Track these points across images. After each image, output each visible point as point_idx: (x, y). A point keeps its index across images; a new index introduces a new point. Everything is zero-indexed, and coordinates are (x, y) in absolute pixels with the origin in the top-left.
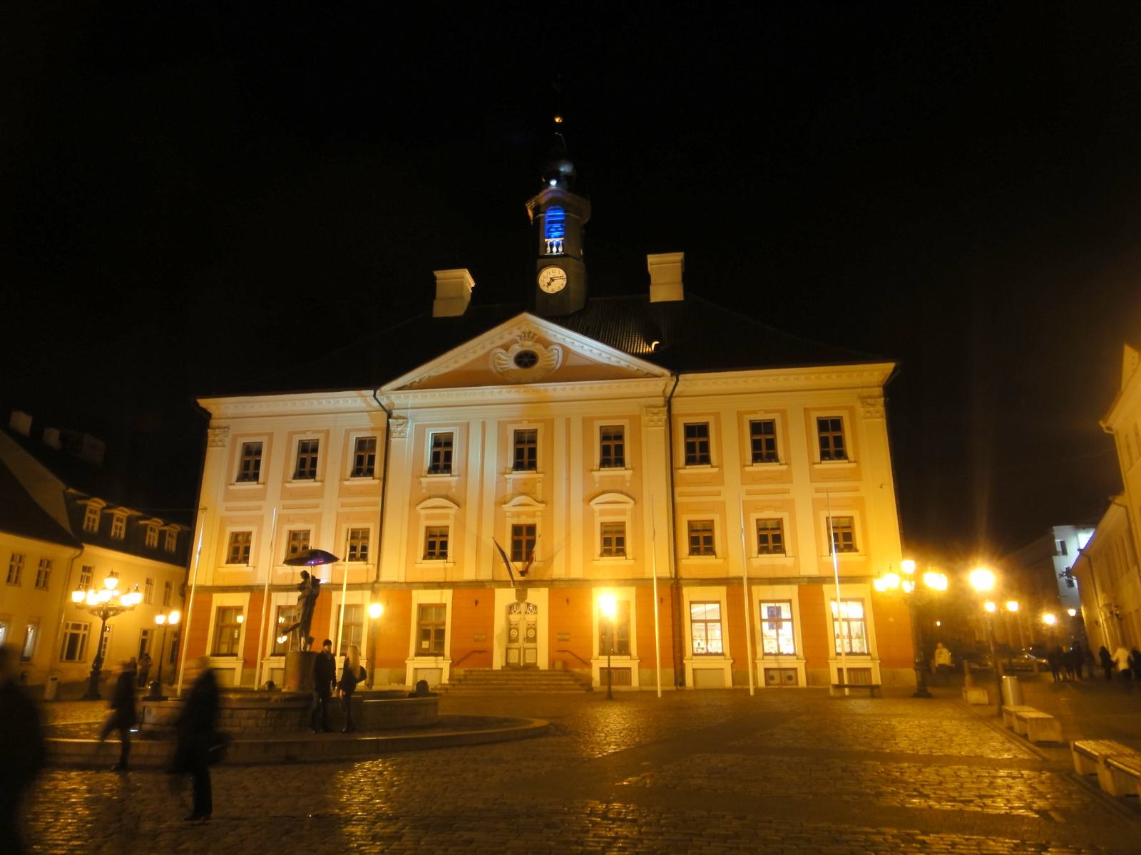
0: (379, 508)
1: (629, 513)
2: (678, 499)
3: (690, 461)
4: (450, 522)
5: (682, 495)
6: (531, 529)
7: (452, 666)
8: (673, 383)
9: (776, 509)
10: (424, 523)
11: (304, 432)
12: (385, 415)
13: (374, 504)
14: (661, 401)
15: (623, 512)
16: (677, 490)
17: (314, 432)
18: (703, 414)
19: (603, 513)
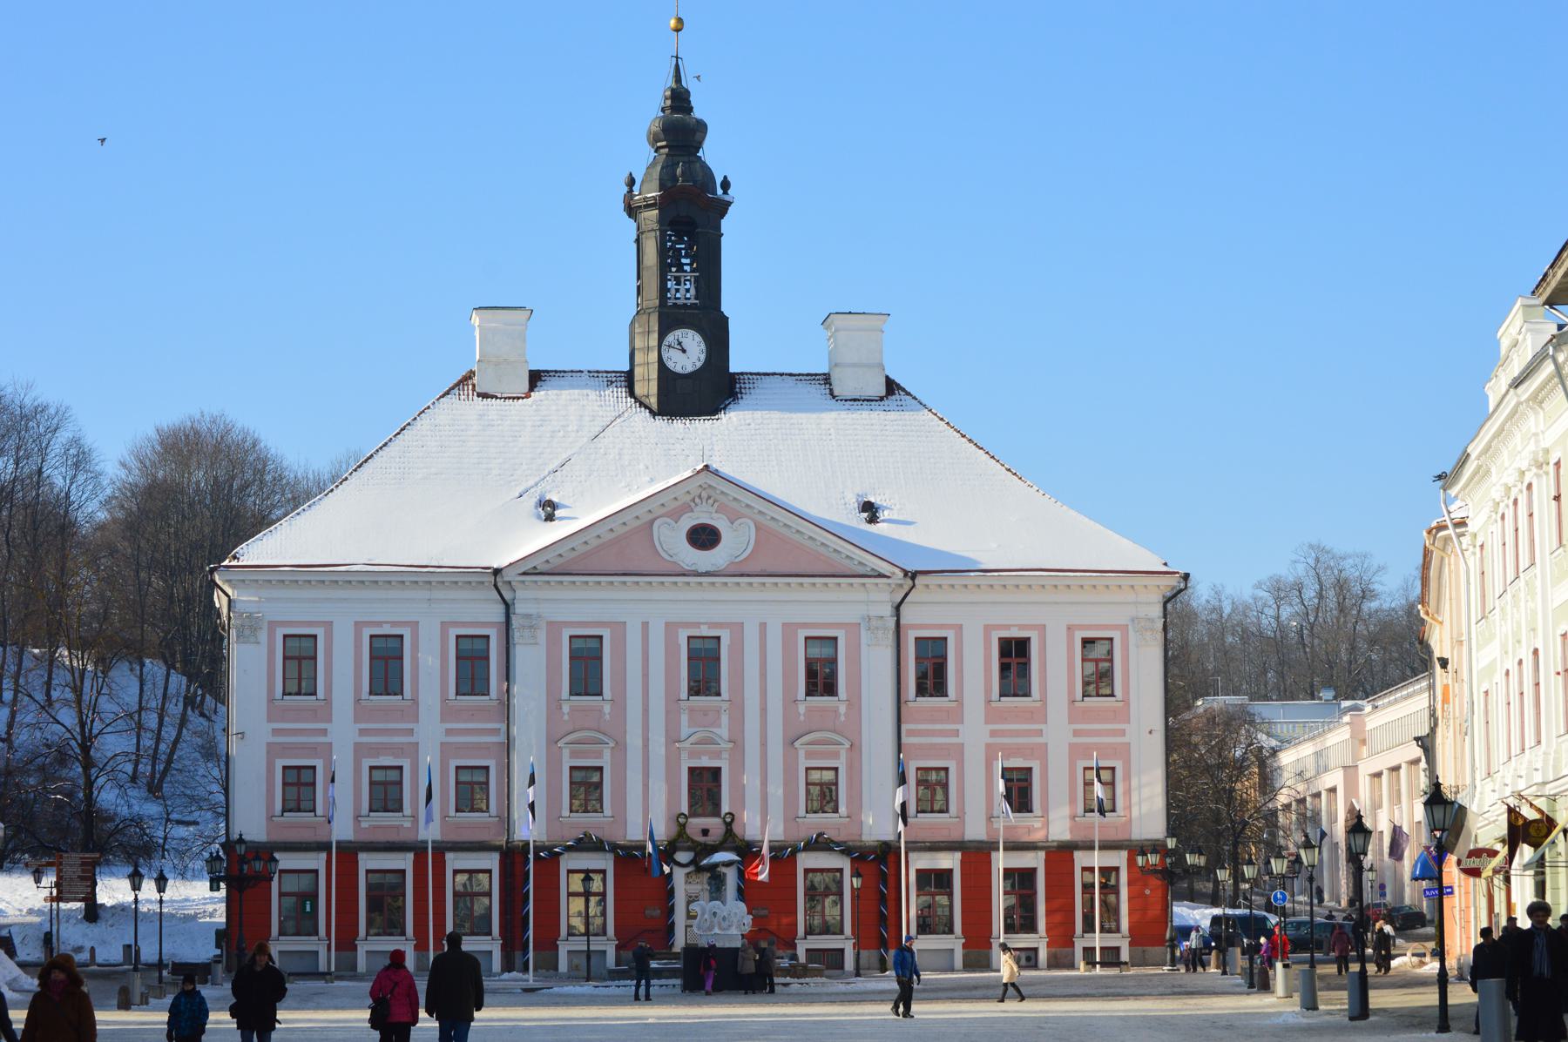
0: (502, 738)
1: (843, 754)
2: (904, 740)
3: (921, 691)
4: (605, 761)
5: (911, 733)
6: (716, 772)
7: (618, 948)
8: (906, 588)
9: (1025, 757)
10: (567, 763)
11: (379, 624)
12: (501, 608)
13: (495, 732)
14: (887, 611)
15: (836, 755)
16: (904, 727)
17: (394, 624)
18: (941, 627)
19: (809, 755)
